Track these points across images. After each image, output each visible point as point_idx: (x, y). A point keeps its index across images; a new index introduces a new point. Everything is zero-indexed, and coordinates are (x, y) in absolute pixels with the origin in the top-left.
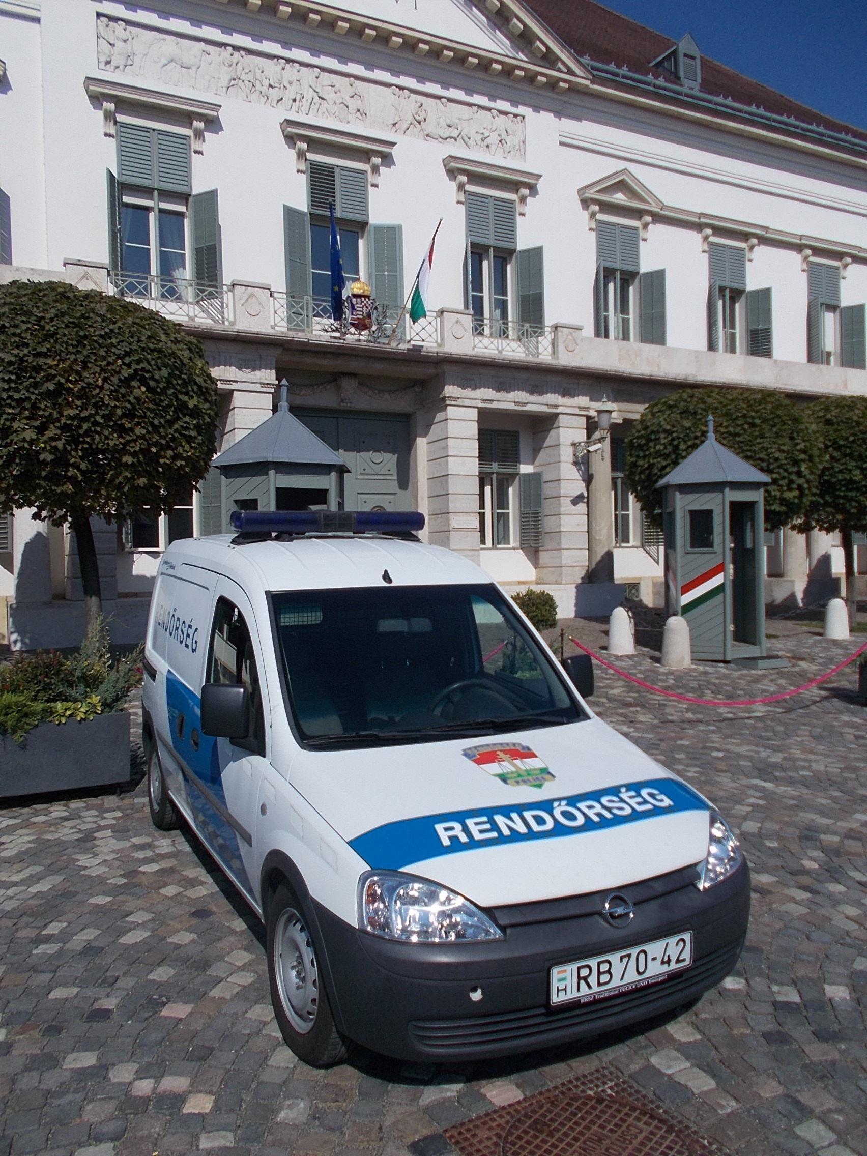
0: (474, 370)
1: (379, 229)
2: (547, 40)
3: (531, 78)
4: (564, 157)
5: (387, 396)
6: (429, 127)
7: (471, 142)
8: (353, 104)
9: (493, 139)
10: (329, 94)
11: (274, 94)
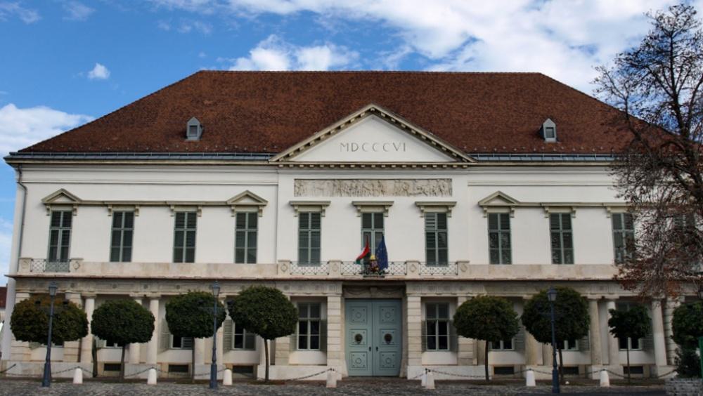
0: (416, 282)
3: (451, 166)
4: (468, 192)
5: (389, 293)
7: (428, 194)
9: (437, 190)
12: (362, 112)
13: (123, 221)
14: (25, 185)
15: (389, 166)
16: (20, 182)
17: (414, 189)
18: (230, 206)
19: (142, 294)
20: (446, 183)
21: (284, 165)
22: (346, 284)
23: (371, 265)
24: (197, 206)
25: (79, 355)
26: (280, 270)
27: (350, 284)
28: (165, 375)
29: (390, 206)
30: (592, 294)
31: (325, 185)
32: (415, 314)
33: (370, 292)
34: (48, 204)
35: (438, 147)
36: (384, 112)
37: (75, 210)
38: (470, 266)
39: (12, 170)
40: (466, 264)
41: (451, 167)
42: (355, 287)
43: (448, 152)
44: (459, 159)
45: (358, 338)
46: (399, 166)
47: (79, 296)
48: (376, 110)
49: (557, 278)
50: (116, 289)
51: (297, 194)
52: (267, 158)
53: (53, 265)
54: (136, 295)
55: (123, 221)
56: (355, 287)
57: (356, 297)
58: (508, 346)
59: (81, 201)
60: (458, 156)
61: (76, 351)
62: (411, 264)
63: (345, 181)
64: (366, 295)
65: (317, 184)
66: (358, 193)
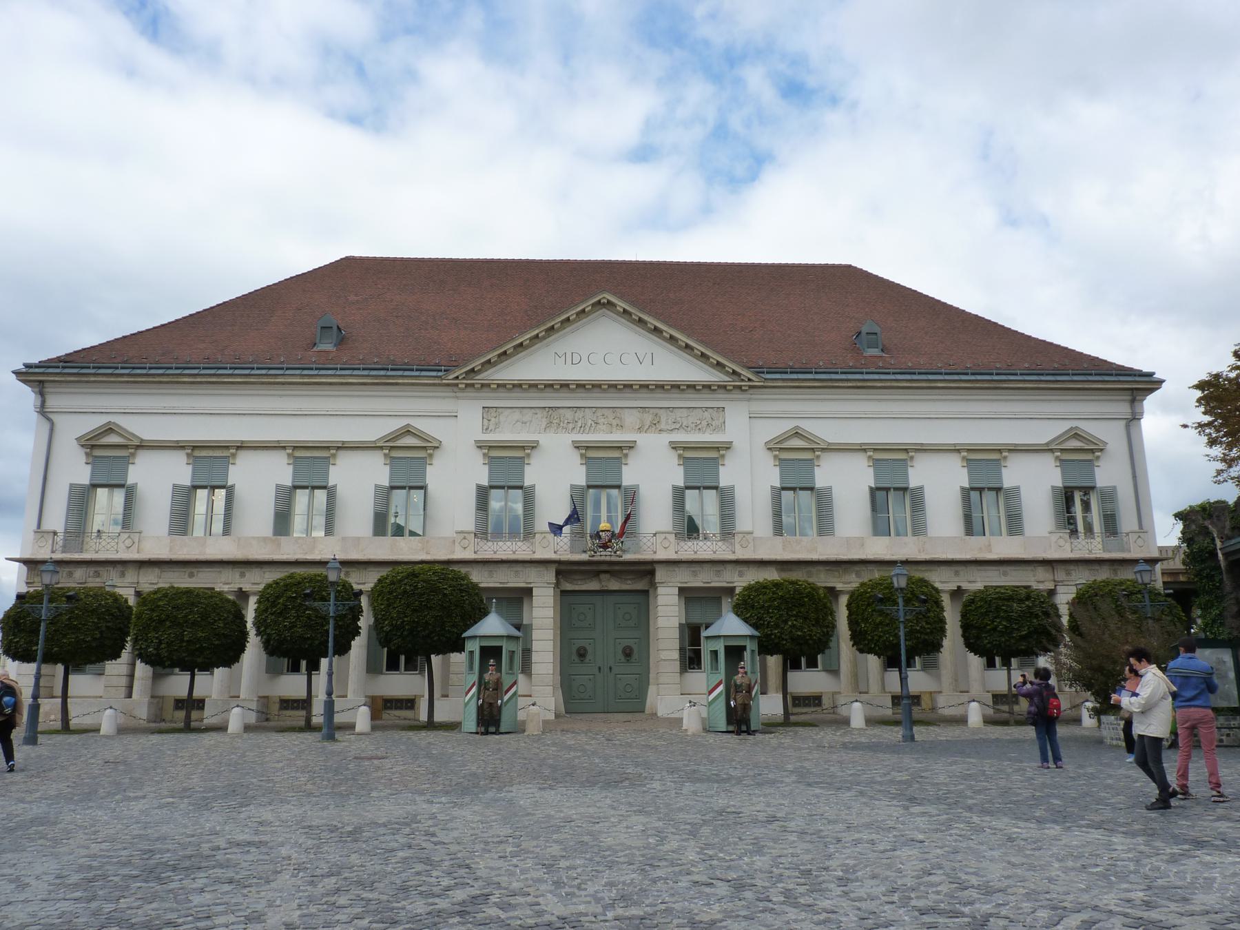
1: (626, 489)
2: (731, 366)
3: (725, 387)
6: (663, 426)
8: (614, 422)
10: (601, 420)
11: (571, 426)
12: (586, 306)
14: (51, 416)
15: (628, 386)
16: (43, 411)
17: (667, 423)
18: (381, 448)
19: (235, 587)
20: (715, 414)
21: (467, 385)
22: (563, 567)
23: (600, 538)
25: (130, 688)
26: (458, 548)
27: (569, 568)
29: (631, 447)
30: (943, 581)
31: (528, 415)
32: (668, 613)
33: (600, 581)
36: (621, 305)
38: (754, 539)
39: (26, 389)
40: (748, 537)
42: (576, 572)
44: (735, 378)
45: (582, 654)
46: (645, 386)
47: (132, 591)
48: (609, 302)
49: (888, 557)
50: (194, 579)
51: (486, 430)
52: (440, 374)
54: (226, 588)
56: (576, 572)
57: (577, 588)
58: (812, 664)
59: (142, 440)
60: (734, 372)
61: (124, 681)
62: (663, 536)
63: (561, 411)
64: (593, 585)
65: (516, 415)
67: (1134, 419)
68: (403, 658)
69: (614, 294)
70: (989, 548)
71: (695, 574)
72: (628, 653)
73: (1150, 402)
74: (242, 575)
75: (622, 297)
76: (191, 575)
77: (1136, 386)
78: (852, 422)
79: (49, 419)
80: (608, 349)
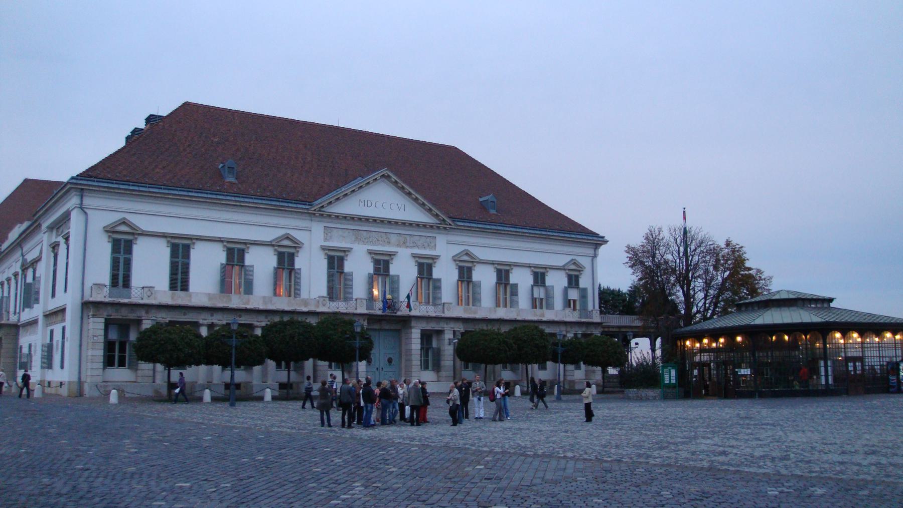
2: (442, 216)
3: (438, 227)
4: (446, 249)
6: (408, 244)
9: (426, 245)
12: (377, 174)
13: (180, 251)
18: (273, 246)
24: (245, 244)
25: (154, 376)
28: (277, 394)
31: (346, 233)
34: (110, 231)
35: (430, 210)
36: (394, 178)
37: (136, 239)
41: (438, 227)
43: (437, 216)
49: (506, 318)
51: (325, 240)
53: (115, 290)
55: (180, 251)
60: (444, 220)
61: (151, 373)
66: (371, 243)
67: (595, 256)
68: (283, 363)
69: (392, 172)
70: (543, 315)
71: (427, 323)
72: (390, 361)
73: (602, 249)
74: (212, 315)
75: (396, 175)
76: (185, 314)
77: (595, 241)
78: (491, 249)
79: (86, 213)
80: (382, 200)
